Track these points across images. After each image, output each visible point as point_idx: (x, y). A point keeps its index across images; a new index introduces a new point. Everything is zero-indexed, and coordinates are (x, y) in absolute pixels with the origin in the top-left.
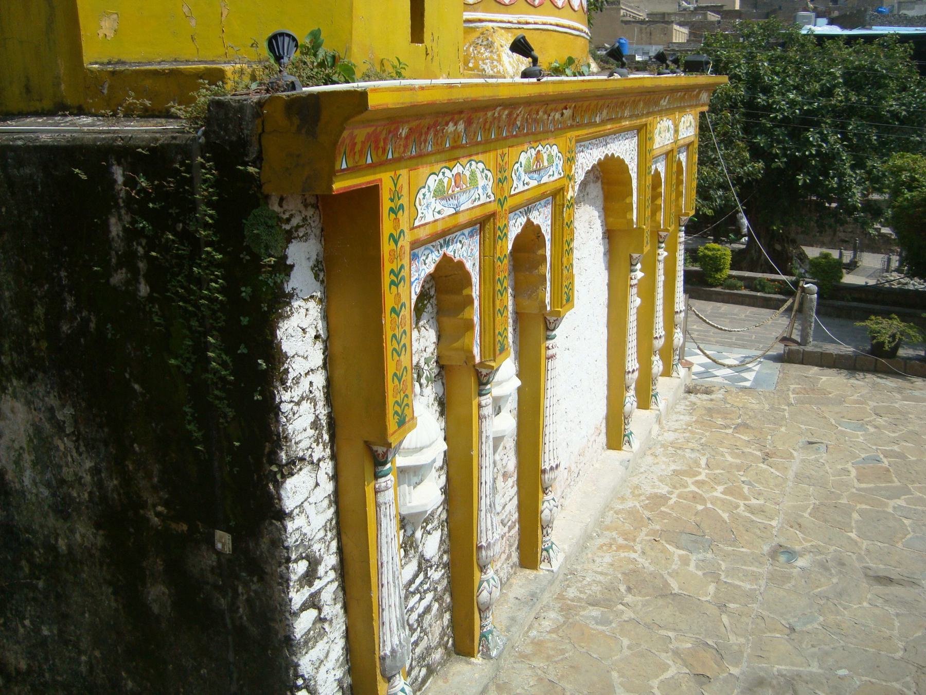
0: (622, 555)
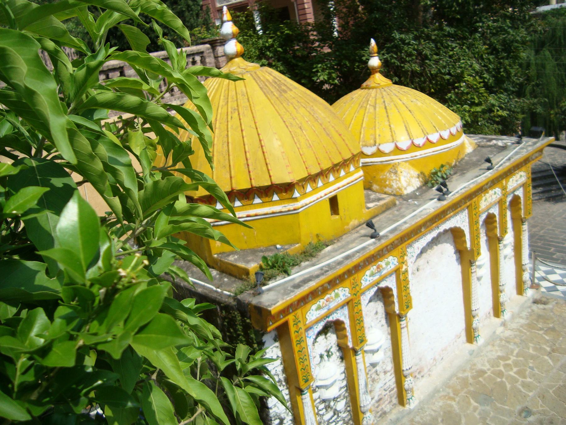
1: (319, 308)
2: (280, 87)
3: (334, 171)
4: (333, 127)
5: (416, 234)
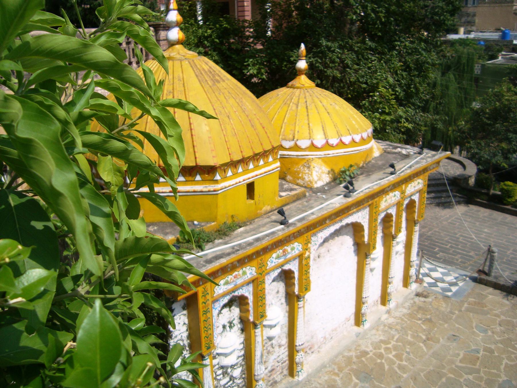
0: (333, 377)
1: (227, 283)
2: (214, 76)
3: (254, 160)
4: (258, 119)
5: (321, 225)
